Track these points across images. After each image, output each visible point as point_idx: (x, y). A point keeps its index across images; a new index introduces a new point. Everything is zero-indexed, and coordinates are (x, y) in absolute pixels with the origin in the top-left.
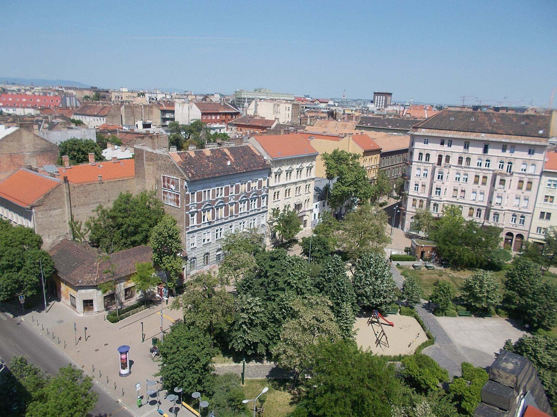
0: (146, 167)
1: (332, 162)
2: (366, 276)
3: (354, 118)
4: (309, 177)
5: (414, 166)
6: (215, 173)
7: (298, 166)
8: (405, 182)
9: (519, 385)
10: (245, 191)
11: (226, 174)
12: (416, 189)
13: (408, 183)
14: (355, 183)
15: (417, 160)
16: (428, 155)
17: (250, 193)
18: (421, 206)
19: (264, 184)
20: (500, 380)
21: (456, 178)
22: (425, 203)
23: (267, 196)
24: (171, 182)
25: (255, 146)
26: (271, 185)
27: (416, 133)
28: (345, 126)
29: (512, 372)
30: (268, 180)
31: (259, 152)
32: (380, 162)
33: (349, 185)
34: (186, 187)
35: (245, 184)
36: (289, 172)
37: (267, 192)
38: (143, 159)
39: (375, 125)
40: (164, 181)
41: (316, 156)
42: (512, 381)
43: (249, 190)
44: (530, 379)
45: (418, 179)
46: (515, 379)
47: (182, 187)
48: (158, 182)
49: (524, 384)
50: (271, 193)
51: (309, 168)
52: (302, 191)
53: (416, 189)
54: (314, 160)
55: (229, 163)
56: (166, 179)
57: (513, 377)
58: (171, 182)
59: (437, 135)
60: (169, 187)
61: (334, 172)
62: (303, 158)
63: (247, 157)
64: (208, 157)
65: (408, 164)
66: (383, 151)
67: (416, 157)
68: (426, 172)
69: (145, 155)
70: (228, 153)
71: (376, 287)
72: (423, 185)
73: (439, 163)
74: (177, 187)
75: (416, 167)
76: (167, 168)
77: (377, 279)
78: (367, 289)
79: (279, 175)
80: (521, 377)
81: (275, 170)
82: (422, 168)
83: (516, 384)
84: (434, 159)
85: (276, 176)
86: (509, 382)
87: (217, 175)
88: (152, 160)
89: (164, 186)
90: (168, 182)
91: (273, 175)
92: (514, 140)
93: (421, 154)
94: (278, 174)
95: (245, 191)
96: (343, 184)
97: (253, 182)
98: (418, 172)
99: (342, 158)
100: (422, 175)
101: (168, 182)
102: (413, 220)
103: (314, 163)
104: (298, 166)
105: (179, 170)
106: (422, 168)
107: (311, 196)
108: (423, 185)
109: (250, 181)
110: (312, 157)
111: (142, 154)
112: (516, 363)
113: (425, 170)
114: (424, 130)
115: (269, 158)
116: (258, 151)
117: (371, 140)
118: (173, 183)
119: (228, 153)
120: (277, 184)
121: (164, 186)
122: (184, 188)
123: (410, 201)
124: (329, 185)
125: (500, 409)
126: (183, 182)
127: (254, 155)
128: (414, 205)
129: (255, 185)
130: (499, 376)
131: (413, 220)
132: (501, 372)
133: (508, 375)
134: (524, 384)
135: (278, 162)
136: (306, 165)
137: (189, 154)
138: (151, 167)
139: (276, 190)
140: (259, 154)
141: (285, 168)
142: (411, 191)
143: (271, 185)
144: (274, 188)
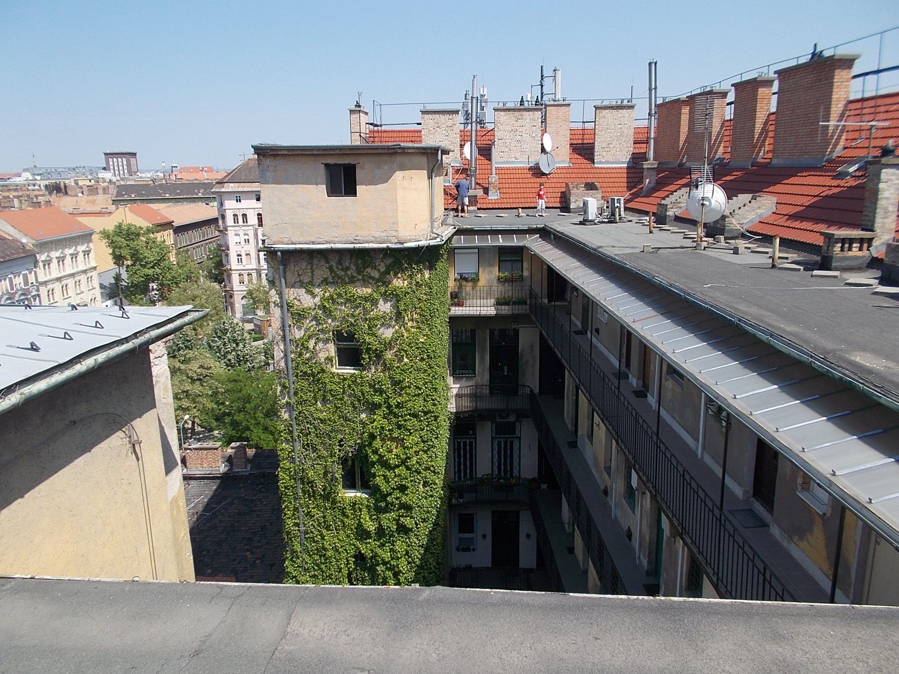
1: (122, 241)
2: (225, 344)
3: (100, 191)
4: (88, 266)
5: (231, 233)
7: (72, 251)
8: (223, 254)
10: (7, 290)
12: (240, 261)
13: (227, 255)
14: (157, 264)
15: (233, 224)
16: (244, 216)
17: (15, 293)
18: (250, 281)
19: (31, 278)
22: (254, 275)
23: (39, 295)
26: (40, 280)
27: (223, 190)
28: (93, 202)
30: (35, 272)
31: (9, 235)
32: (175, 240)
33: (153, 267)
35: (5, 280)
36: (61, 259)
37: (38, 290)
39: (143, 195)
41: (91, 234)
43: (12, 289)
45: (239, 248)
50: (43, 291)
51: (87, 253)
52: (84, 286)
53: (240, 261)
54: (91, 241)
59: (249, 190)
61: (125, 252)
62: (74, 238)
65: (223, 232)
66: (175, 224)
67: (230, 221)
68: (246, 237)
71: (239, 353)
72: (247, 255)
73: (261, 224)
75: (233, 233)
77: (237, 345)
78: (229, 357)
79: (49, 264)
81: (41, 257)
82: (241, 233)
84: (253, 220)
85: (44, 266)
91: (41, 264)
93: (235, 215)
94: (47, 263)
95: (7, 290)
96: (144, 266)
97: (15, 277)
98: (237, 239)
99: (132, 233)
100: (243, 242)
102: (244, 302)
103: (91, 245)
104: (72, 251)
106: (241, 233)
107: (98, 292)
108: (247, 255)
109: (12, 276)
110: (86, 237)
113: (245, 234)
114: (232, 185)
115: (30, 240)
116: (5, 233)
117: (156, 212)
120: (48, 278)
123: (235, 278)
124: (120, 274)
128: (242, 282)
129: (19, 281)
131: (244, 302)
135: (45, 246)
136: (82, 248)
139: (50, 287)
141: (55, 254)
142: (234, 264)
143: (40, 280)
144: (45, 283)
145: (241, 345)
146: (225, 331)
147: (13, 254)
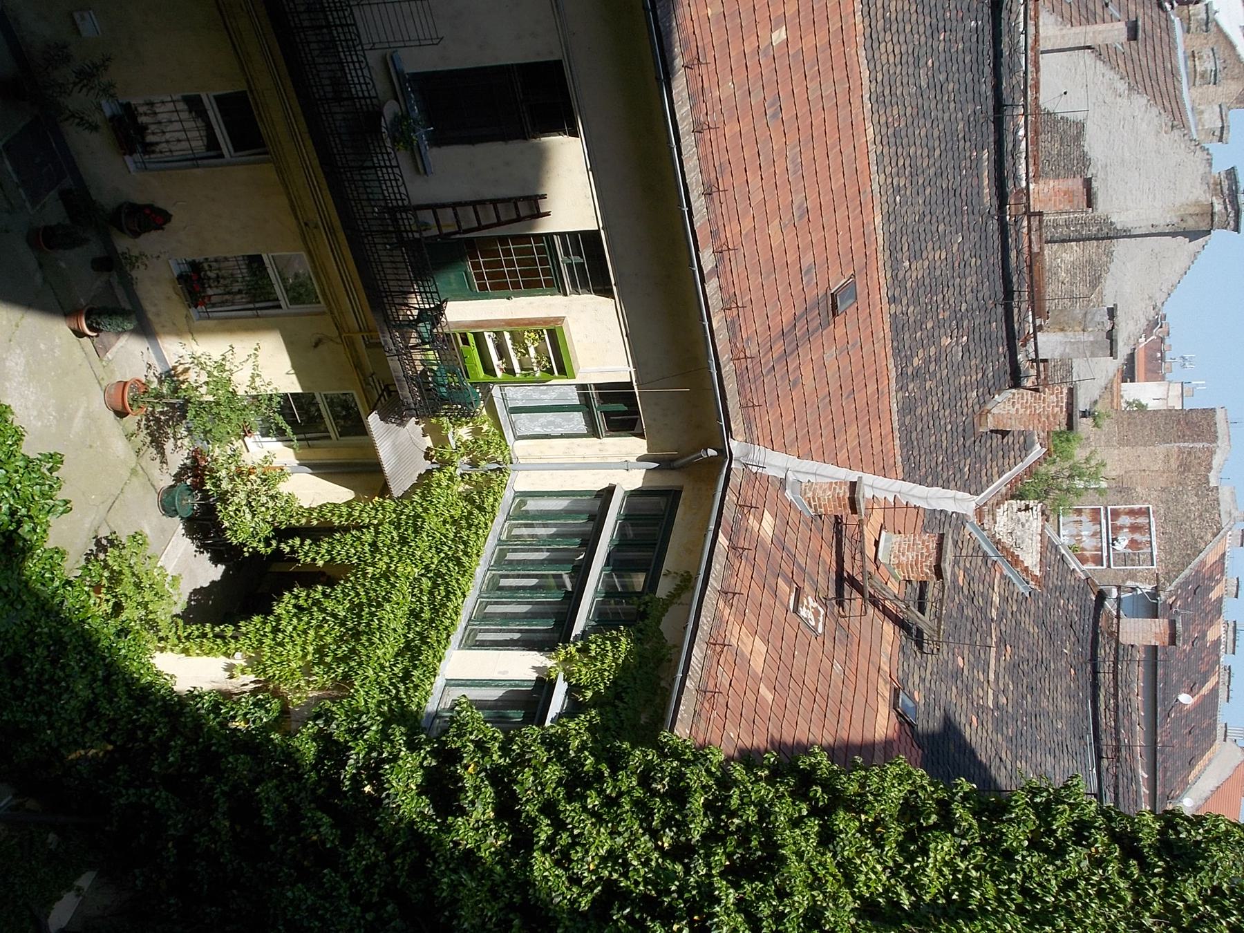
0: (1161, 449)
6: (1165, 667)
11: (1160, 696)
24: (1137, 536)
25: (1215, 763)
31: (1198, 777)
34: (1134, 589)
38: (1182, 438)
40: (1131, 513)
47: (1132, 576)
48: (1123, 489)
55: (1184, 698)
56: (1141, 520)
58: (1137, 536)
60: (1117, 529)
63: (1188, 744)
64: (1204, 635)
69: (1199, 445)
70: (1205, 690)
74: (1125, 559)
76: (1179, 525)
87: (1160, 671)
88: (1184, 467)
89: (1116, 514)
90: (1134, 528)
101: (1134, 528)
105: (1185, 565)
111: (1199, 437)
116: (1201, 772)
118: (1133, 543)
119: (1205, 690)
121: (1116, 514)
122: (1130, 583)
126: (1146, 579)
127: (1191, 763)
137: (1218, 582)
138: (1159, 466)
140: (1191, 778)
147: (1165, 770)
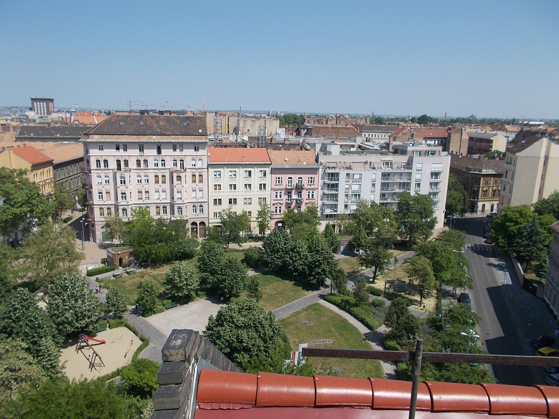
2: (64, 301)
3: (11, 129)
5: (94, 174)
8: (87, 191)
9: (189, 356)
12: (101, 197)
13: (91, 193)
14: (27, 202)
15: (95, 167)
16: (106, 162)
18: (109, 214)
20: (172, 359)
21: (106, 181)
22: (113, 210)
27: (88, 140)
29: (181, 346)
33: (21, 206)
39: (40, 135)
42: (182, 355)
44: (199, 346)
45: (100, 187)
46: (183, 352)
49: (194, 353)
53: (101, 197)
57: (182, 351)
59: (110, 141)
65: (87, 172)
66: (55, 162)
67: (93, 165)
68: (107, 179)
71: (77, 309)
72: (107, 193)
73: (119, 168)
75: (96, 175)
77: (76, 301)
78: (67, 315)
80: (188, 349)
82: (103, 175)
83: (185, 356)
84: (113, 165)
86: (180, 357)
92: (144, 139)
93: (98, 161)
96: (13, 206)
98: (99, 180)
100: (104, 183)
102: (104, 230)
106: (103, 175)
112: (184, 337)
113: (106, 177)
114: (96, 136)
123: (97, 211)
125: (176, 384)
130: (171, 355)
131: (104, 230)
132: (171, 351)
133: (177, 351)
134: (194, 353)
142: (96, 200)
145: (80, 302)
146: (65, 288)
